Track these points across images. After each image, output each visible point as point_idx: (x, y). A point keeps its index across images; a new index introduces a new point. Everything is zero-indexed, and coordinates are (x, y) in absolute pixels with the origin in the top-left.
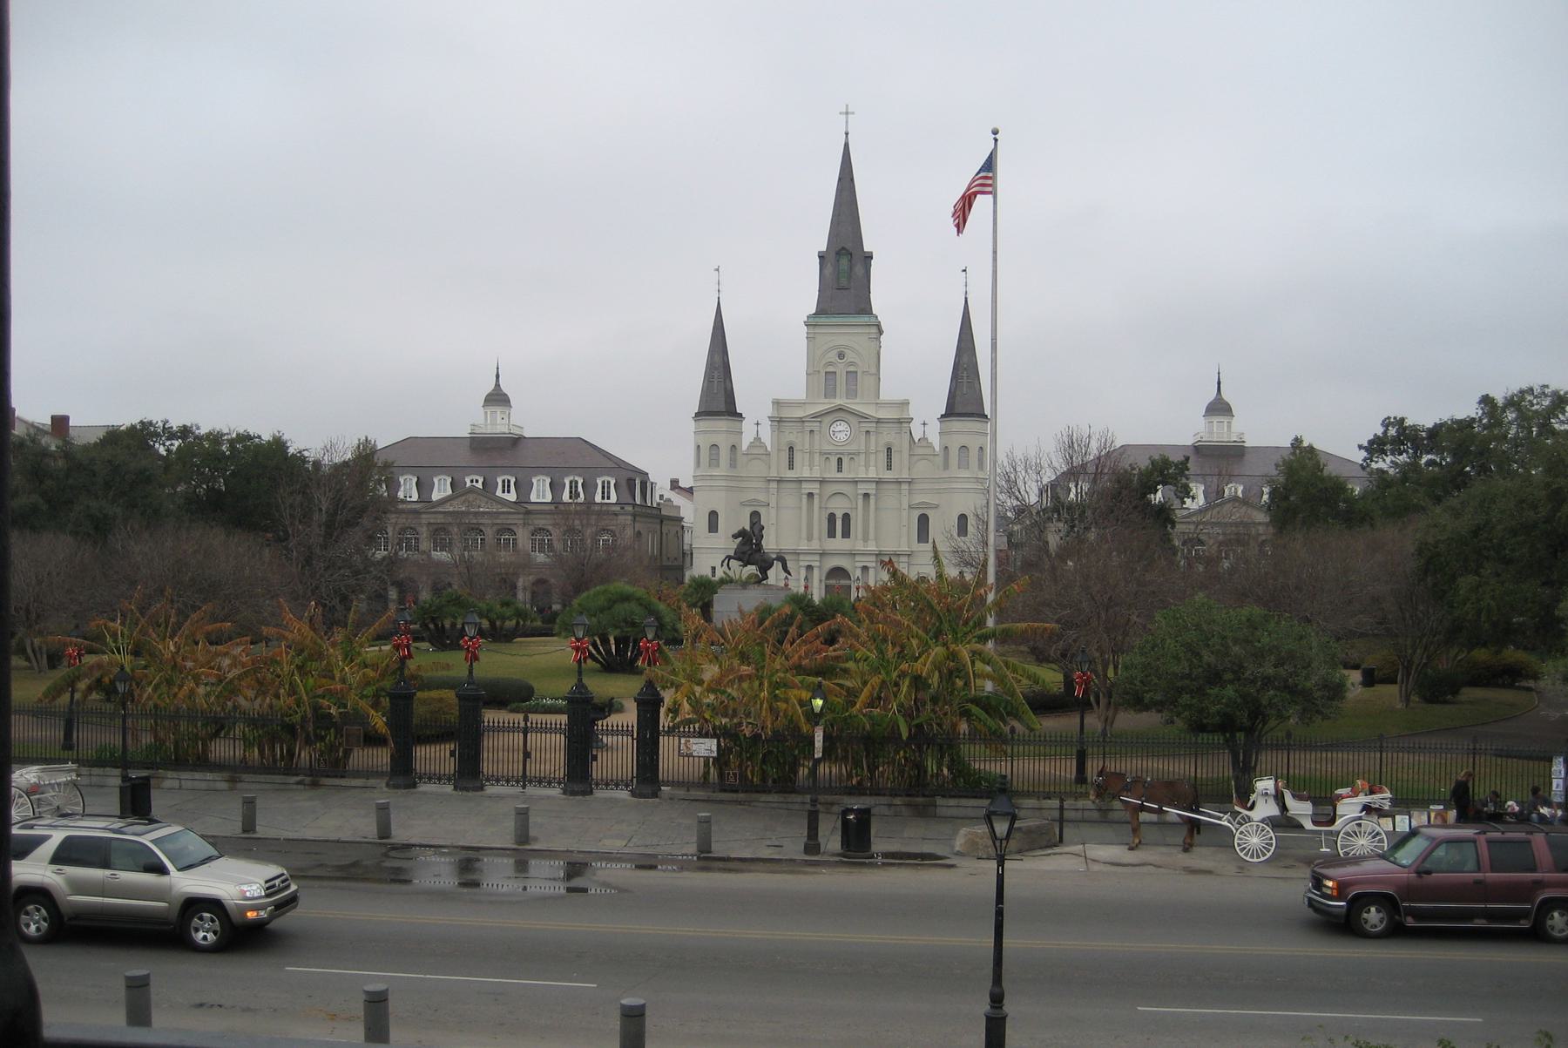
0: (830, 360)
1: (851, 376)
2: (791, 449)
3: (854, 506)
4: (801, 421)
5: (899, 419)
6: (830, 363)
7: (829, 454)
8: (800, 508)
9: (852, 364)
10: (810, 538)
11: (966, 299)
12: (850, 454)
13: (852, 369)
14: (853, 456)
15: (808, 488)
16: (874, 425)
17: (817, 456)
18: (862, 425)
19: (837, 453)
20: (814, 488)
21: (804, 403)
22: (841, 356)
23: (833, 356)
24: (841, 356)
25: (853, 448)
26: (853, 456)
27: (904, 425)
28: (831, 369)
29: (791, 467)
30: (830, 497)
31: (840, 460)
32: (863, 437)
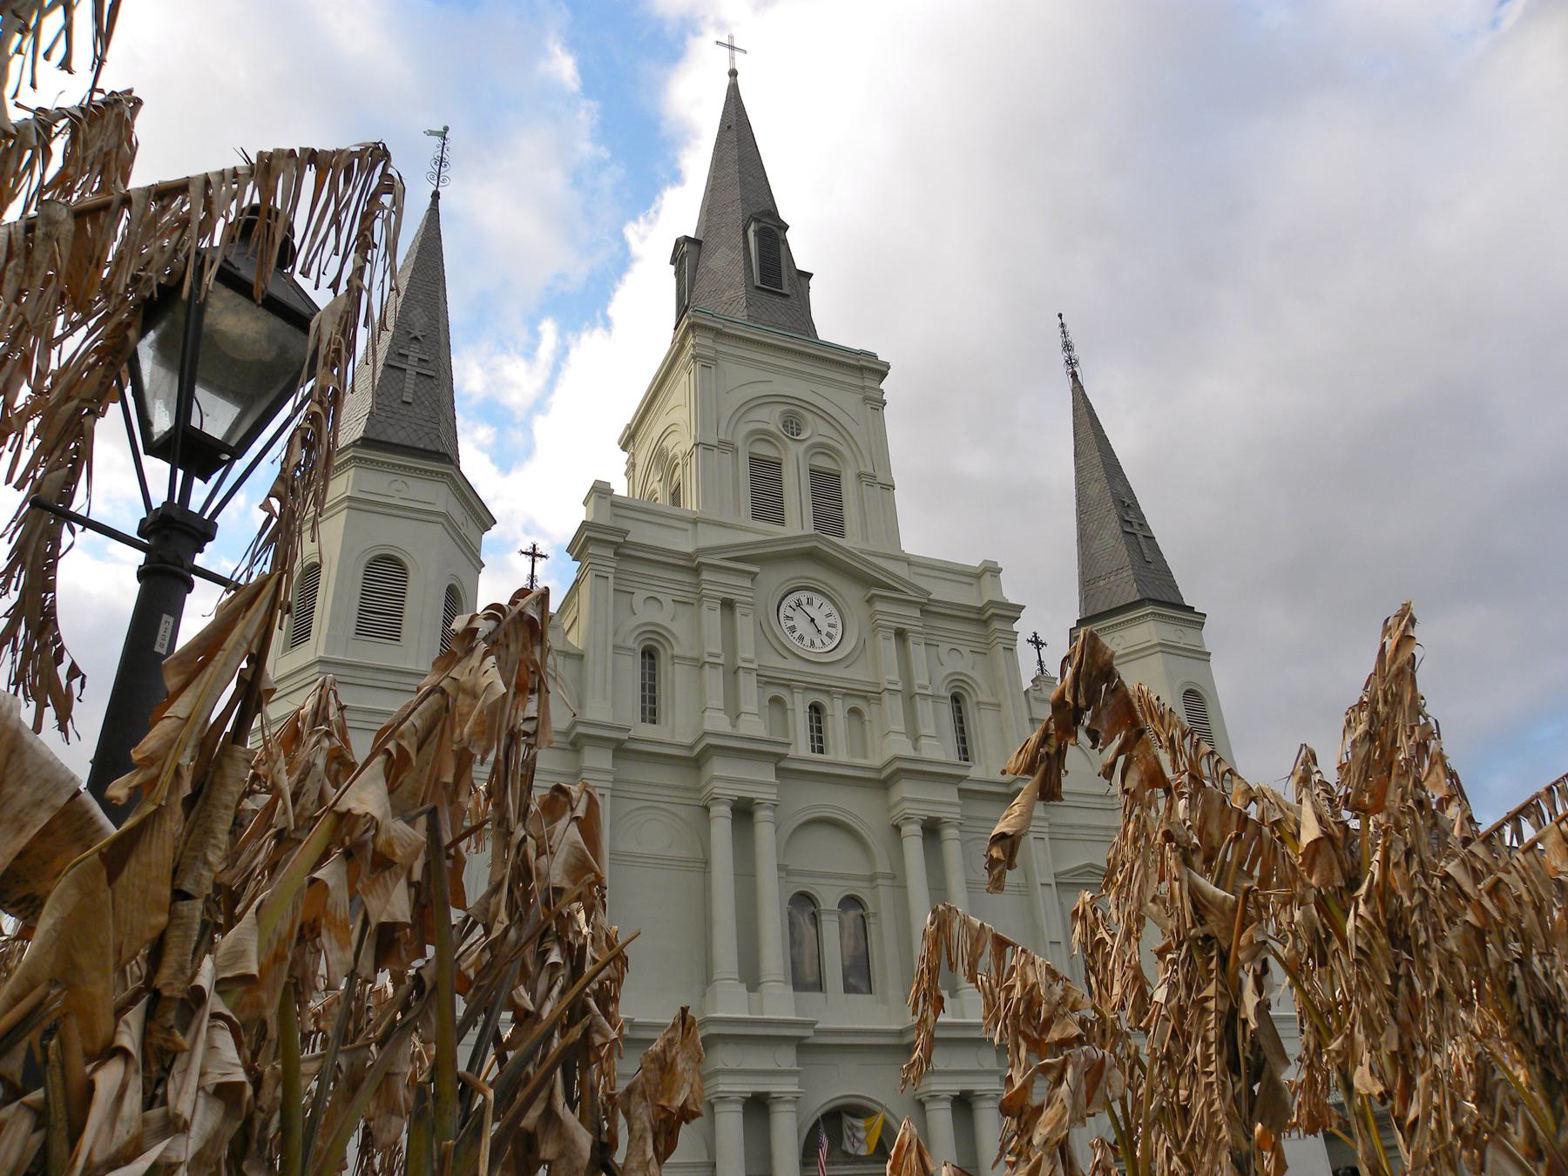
0: (765, 426)
1: (825, 485)
2: (649, 654)
3: (883, 866)
4: (692, 566)
5: (980, 610)
6: (762, 436)
7: (787, 685)
8: (706, 863)
9: (823, 449)
10: (751, 977)
11: (1074, 375)
12: (848, 694)
13: (823, 463)
14: (862, 699)
15: (728, 779)
16: (917, 613)
17: (748, 684)
18: (879, 606)
19: (810, 688)
20: (757, 781)
21: (695, 522)
22: (792, 425)
23: (770, 418)
24: (792, 425)
25: (858, 674)
26: (862, 699)
27: (996, 625)
28: (765, 450)
29: (650, 713)
30: (793, 833)
31: (816, 710)
32: (890, 647)
